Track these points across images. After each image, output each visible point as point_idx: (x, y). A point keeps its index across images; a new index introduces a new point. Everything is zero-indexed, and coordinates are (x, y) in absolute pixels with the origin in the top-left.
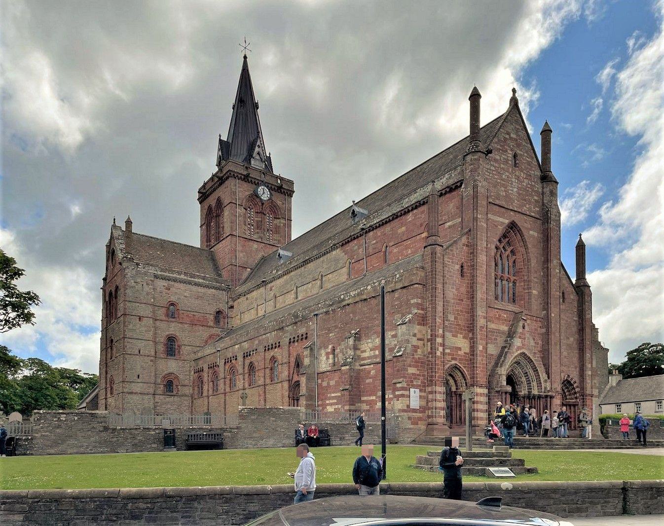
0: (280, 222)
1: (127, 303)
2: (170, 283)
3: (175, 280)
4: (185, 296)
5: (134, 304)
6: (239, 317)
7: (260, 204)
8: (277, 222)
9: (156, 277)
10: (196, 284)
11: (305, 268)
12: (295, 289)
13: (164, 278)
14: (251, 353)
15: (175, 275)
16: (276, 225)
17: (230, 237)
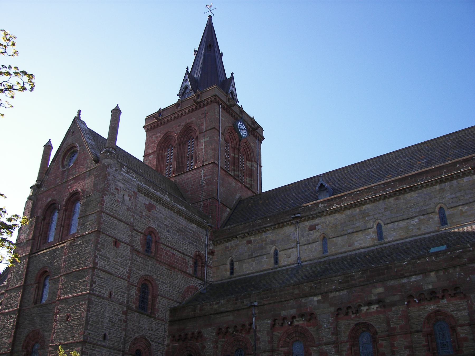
0: (252, 166)
1: (103, 214)
2: (153, 202)
3: (158, 200)
4: (166, 225)
5: (111, 218)
6: (228, 266)
7: (237, 140)
8: (249, 164)
9: (140, 190)
10: (179, 213)
11: (397, 199)
12: (375, 226)
13: (147, 194)
14: (364, 309)
15: (159, 194)
16: (248, 167)
17: (211, 165)
